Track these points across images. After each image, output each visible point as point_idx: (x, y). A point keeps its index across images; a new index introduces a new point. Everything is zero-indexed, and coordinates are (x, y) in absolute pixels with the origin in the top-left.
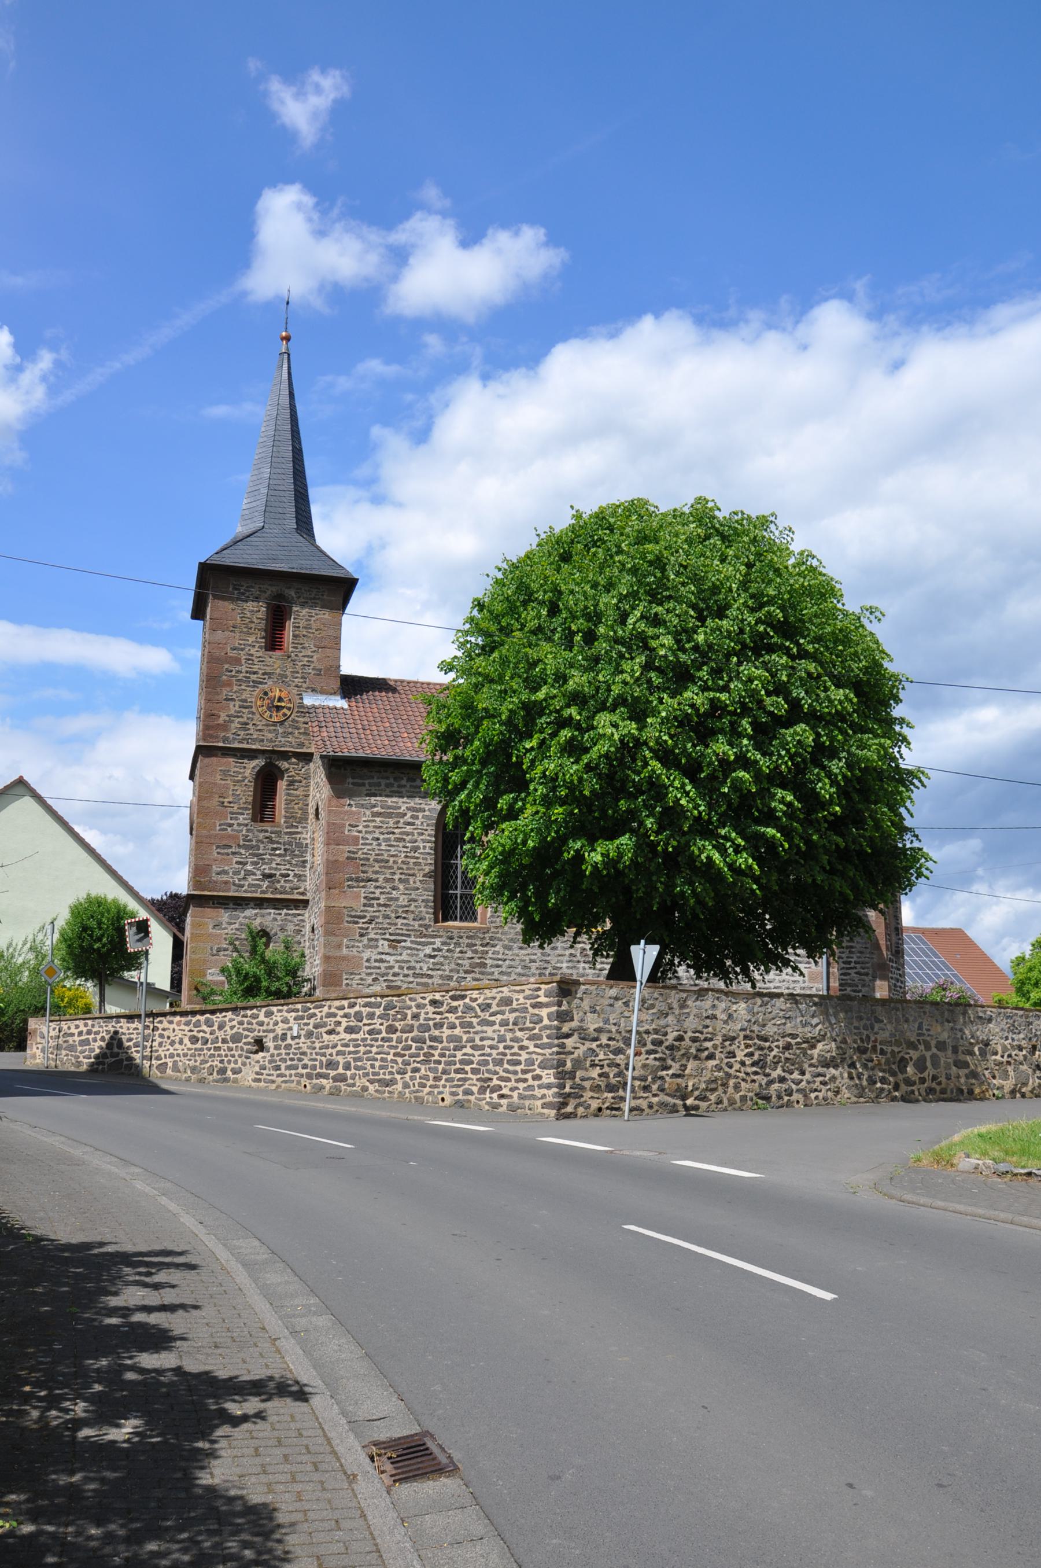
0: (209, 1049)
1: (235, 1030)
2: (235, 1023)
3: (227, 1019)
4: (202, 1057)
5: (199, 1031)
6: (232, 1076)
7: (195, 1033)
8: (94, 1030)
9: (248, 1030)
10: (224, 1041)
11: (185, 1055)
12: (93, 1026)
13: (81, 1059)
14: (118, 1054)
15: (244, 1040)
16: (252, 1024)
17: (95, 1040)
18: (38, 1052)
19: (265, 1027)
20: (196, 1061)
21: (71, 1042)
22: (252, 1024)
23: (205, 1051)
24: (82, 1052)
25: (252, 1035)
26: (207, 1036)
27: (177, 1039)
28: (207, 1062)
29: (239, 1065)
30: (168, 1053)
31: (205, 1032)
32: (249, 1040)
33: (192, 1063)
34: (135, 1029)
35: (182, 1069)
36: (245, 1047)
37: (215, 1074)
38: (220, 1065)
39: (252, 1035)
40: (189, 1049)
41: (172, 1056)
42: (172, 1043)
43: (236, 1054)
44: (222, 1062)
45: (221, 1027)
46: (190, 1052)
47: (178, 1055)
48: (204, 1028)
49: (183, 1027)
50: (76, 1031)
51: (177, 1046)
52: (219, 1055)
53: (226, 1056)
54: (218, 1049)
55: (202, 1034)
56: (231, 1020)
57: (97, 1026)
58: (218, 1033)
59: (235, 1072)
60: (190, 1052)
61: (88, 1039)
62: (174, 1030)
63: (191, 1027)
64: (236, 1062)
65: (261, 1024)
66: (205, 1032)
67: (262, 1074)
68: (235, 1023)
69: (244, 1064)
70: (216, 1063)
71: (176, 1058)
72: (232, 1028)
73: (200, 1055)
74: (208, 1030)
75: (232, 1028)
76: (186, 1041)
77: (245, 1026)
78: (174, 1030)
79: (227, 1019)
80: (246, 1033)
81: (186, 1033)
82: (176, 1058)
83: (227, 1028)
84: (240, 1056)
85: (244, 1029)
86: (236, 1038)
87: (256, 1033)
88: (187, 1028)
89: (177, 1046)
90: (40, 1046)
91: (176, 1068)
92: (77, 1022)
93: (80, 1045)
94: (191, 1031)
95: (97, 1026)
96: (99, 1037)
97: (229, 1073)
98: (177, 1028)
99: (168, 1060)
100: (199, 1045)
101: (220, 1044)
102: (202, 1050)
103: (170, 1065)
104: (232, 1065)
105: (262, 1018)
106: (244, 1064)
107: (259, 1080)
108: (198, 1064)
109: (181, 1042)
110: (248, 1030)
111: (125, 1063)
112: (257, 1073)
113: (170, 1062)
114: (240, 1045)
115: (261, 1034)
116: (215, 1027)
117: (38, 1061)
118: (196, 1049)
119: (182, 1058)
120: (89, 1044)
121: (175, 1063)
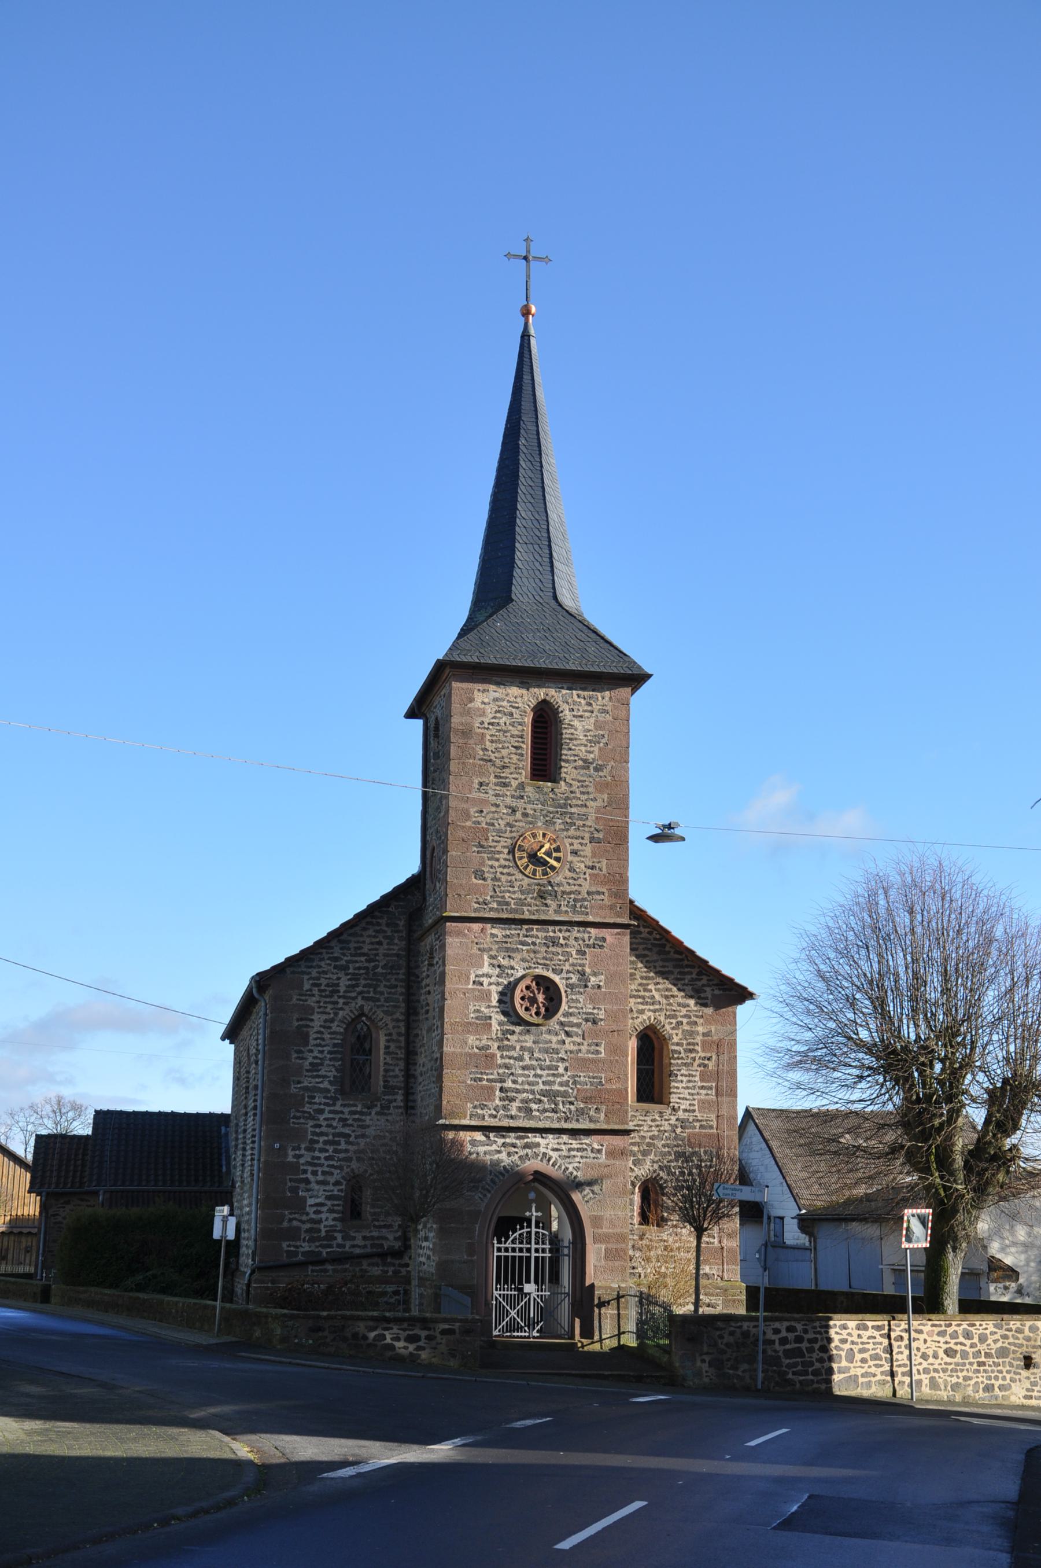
0: (971, 1364)
1: (999, 1344)
2: (997, 1337)
3: (988, 1332)
4: (965, 1373)
5: (956, 1344)
6: (1001, 1394)
7: (952, 1345)
8: (806, 1337)
9: (1015, 1345)
10: (988, 1355)
11: (944, 1371)
12: (806, 1331)
13: (790, 1376)
14: (848, 1369)
15: (1011, 1356)
16: (1018, 1338)
17: (811, 1350)
18: (705, 1367)
19: (1032, 1343)
20: (958, 1377)
21: (770, 1352)
22: (1018, 1338)
23: (968, 1366)
24: (789, 1366)
25: (1020, 1350)
26: (967, 1349)
27: (930, 1352)
28: (970, 1378)
29: (1008, 1381)
30: (921, 1368)
31: (965, 1345)
32: (1018, 1355)
33: (954, 1380)
34: (869, 1338)
35: (942, 1387)
36: (1015, 1363)
37: (981, 1391)
38: (986, 1382)
39: (1020, 1350)
40: (946, 1363)
41: (926, 1371)
42: (925, 1357)
43: (1004, 1370)
44: (989, 1378)
45: (983, 1339)
46: (950, 1367)
47: (936, 1371)
48: (961, 1339)
49: (936, 1338)
50: (776, 1337)
51: (931, 1360)
52: (985, 1371)
53: (993, 1371)
54: (981, 1364)
55: (958, 1348)
56: (992, 1333)
57: (811, 1331)
58: (979, 1347)
59: (1001, 1388)
60: (950, 1367)
61: (799, 1349)
62: (925, 1341)
63: (947, 1338)
64: (1004, 1378)
65: (1028, 1339)
66: (965, 1345)
67: (1033, 1391)
68: (997, 1337)
69: (1012, 1380)
70: (980, 1380)
71: (933, 1374)
72: (995, 1341)
73: (962, 1371)
74: (968, 1342)
75: (995, 1341)
76: (941, 1354)
77: (1011, 1340)
78: (925, 1341)
79: (988, 1332)
80: (1013, 1348)
81: (941, 1344)
82: (933, 1374)
83: (990, 1341)
84: (1008, 1372)
85: (1009, 1344)
86: (1003, 1352)
87: (1025, 1349)
88: (942, 1340)
89: (931, 1360)
90: (707, 1358)
91: (934, 1384)
92: (777, 1325)
93: (787, 1357)
94: (946, 1343)
95: (811, 1331)
96: (817, 1346)
97: (996, 1389)
98: (929, 1339)
99: (923, 1376)
100: (958, 1359)
101: (983, 1359)
102: (964, 1364)
103: (926, 1382)
104: (1001, 1382)
105: (1027, 1332)
106: (1012, 1380)
107: (1031, 1397)
108: (961, 1380)
109: (935, 1356)
110: (1015, 1345)
111: (861, 1380)
112: (1028, 1390)
113: (925, 1379)
114: (1007, 1360)
115: (1030, 1350)
116: (976, 1340)
117: (706, 1380)
118: (957, 1364)
119: (941, 1374)
120: (803, 1356)
121: (932, 1379)
